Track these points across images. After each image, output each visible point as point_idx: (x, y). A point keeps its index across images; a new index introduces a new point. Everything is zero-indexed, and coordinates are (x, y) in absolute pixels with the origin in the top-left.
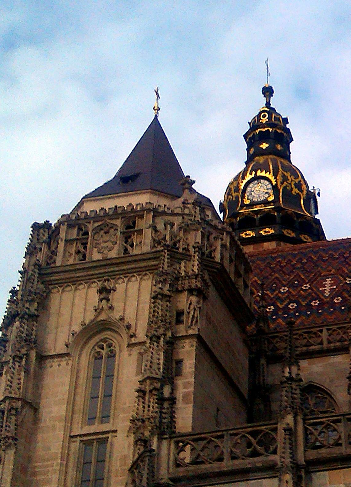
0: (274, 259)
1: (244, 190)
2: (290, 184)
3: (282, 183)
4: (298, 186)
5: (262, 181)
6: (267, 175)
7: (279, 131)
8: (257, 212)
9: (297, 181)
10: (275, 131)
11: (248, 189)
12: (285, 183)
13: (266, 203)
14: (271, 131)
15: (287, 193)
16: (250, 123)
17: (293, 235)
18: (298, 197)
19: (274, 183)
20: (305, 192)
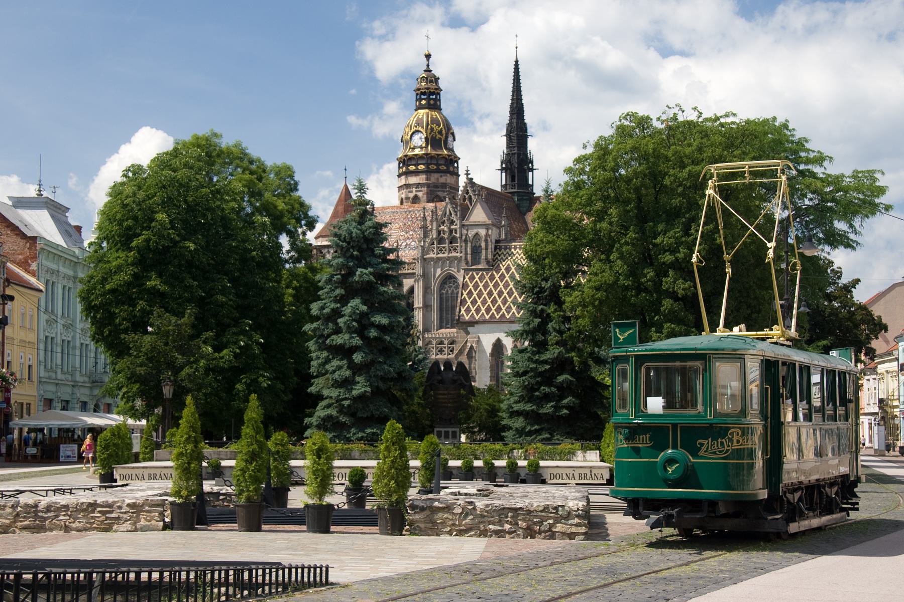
0: (410, 212)
6: (422, 130)
8: (416, 155)
11: (413, 138)
13: (421, 148)
15: (433, 139)
17: (435, 167)
18: (440, 139)
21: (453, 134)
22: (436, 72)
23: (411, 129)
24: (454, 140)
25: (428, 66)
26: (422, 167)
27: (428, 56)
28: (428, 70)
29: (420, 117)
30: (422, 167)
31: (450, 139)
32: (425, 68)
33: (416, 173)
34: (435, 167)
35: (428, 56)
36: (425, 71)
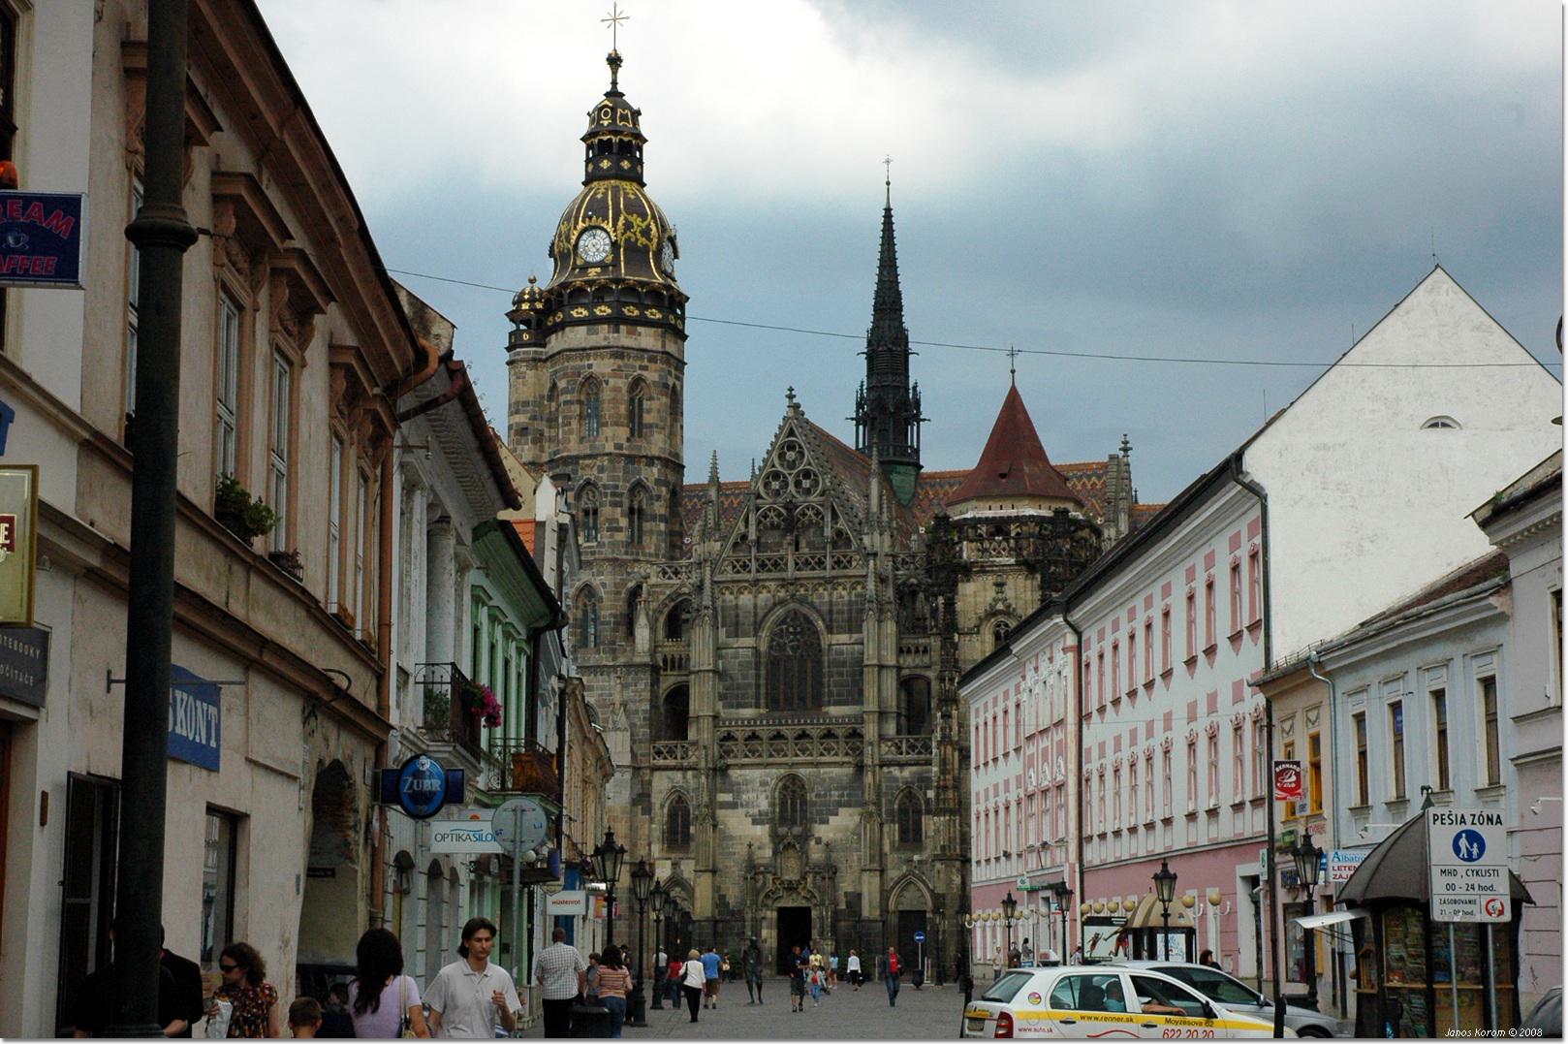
1: (576, 246)
2: (635, 233)
3: (623, 234)
4: (646, 232)
5: (599, 232)
6: (604, 225)
7: (626, 139)
8: (590, 283)
9: (644, 225)
10: (621, 140)
11: (581, 243)
12: (628, 233)
13: (602, 265)
14: (614, 139)
15: (631, 247)
16: (589, 114)
17: (636, 313)
18: (646, 249)
19: (613, 239)
20: (655, 240)
21: (672, 240)
22: (632, 99)
23: (576, 223)
24: (676, 256)
25: (614, 83)
26: (603, 311)
27: (614, 61)
28: (614, 94)
29: (599, 196)
30: (603, 311)
31: (668, 251)
32: (609, 88)
33: (592, 322)
34: (636, 313)
35: (614, 61)
36: (607, 95)
